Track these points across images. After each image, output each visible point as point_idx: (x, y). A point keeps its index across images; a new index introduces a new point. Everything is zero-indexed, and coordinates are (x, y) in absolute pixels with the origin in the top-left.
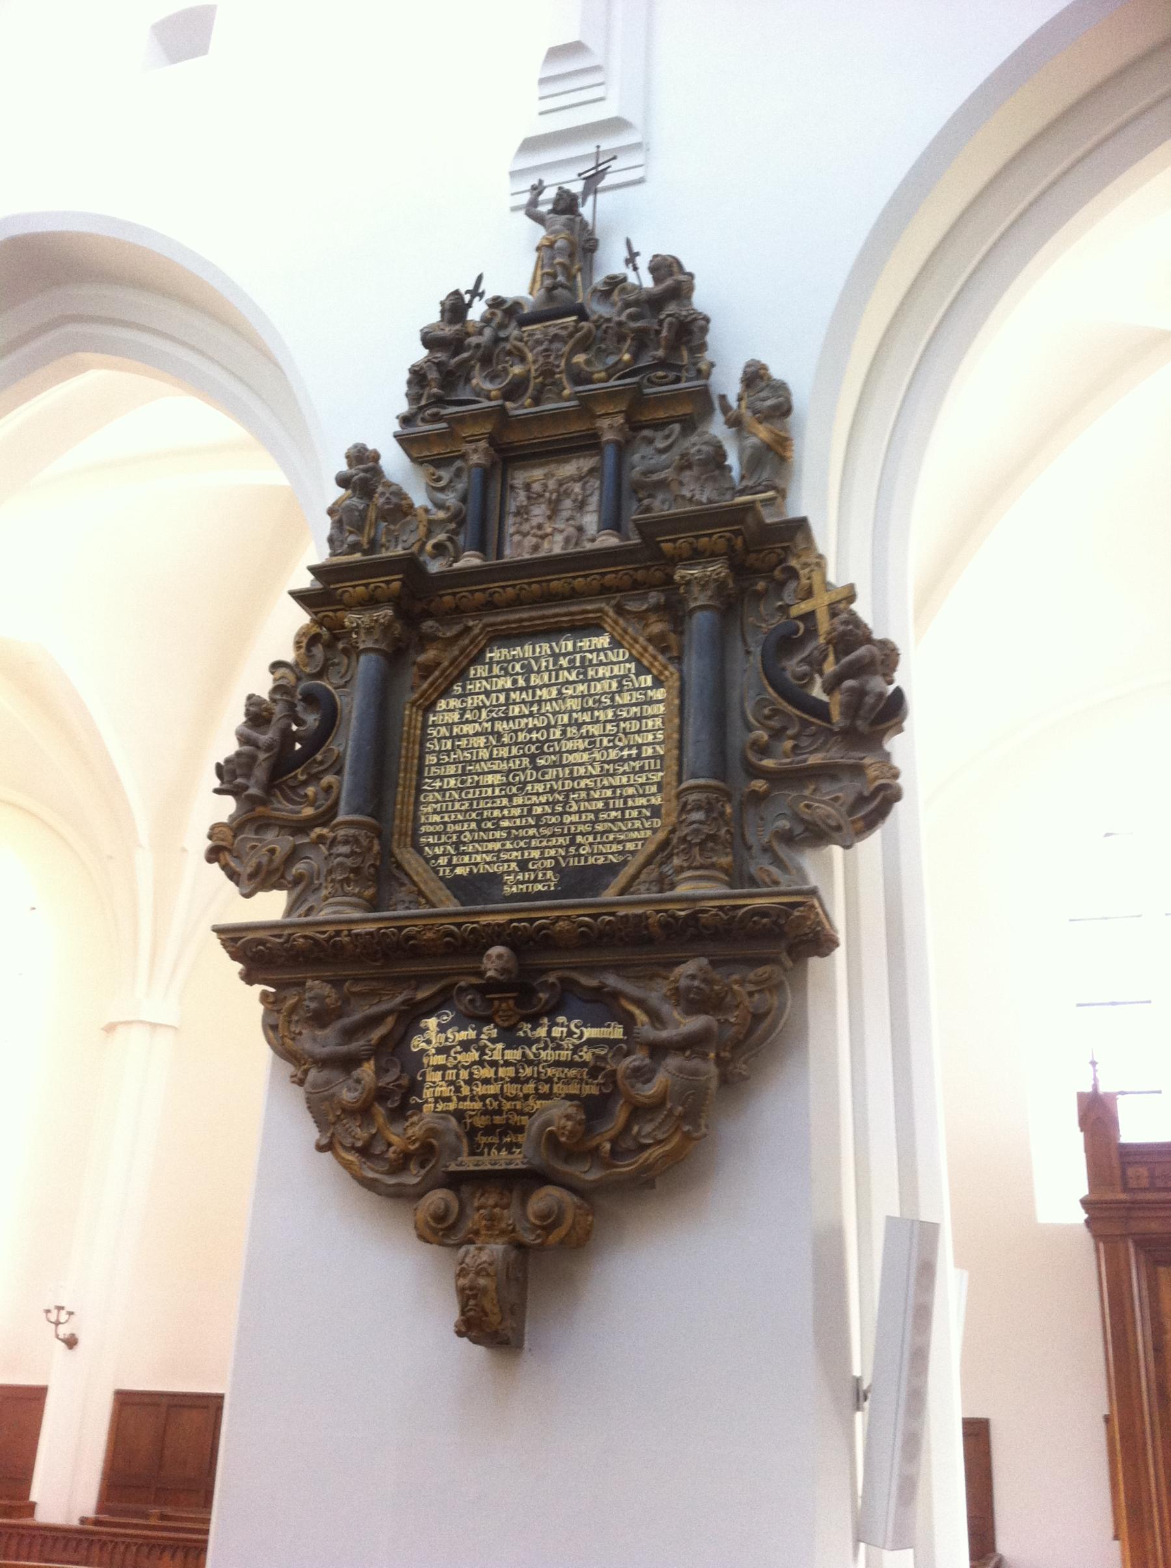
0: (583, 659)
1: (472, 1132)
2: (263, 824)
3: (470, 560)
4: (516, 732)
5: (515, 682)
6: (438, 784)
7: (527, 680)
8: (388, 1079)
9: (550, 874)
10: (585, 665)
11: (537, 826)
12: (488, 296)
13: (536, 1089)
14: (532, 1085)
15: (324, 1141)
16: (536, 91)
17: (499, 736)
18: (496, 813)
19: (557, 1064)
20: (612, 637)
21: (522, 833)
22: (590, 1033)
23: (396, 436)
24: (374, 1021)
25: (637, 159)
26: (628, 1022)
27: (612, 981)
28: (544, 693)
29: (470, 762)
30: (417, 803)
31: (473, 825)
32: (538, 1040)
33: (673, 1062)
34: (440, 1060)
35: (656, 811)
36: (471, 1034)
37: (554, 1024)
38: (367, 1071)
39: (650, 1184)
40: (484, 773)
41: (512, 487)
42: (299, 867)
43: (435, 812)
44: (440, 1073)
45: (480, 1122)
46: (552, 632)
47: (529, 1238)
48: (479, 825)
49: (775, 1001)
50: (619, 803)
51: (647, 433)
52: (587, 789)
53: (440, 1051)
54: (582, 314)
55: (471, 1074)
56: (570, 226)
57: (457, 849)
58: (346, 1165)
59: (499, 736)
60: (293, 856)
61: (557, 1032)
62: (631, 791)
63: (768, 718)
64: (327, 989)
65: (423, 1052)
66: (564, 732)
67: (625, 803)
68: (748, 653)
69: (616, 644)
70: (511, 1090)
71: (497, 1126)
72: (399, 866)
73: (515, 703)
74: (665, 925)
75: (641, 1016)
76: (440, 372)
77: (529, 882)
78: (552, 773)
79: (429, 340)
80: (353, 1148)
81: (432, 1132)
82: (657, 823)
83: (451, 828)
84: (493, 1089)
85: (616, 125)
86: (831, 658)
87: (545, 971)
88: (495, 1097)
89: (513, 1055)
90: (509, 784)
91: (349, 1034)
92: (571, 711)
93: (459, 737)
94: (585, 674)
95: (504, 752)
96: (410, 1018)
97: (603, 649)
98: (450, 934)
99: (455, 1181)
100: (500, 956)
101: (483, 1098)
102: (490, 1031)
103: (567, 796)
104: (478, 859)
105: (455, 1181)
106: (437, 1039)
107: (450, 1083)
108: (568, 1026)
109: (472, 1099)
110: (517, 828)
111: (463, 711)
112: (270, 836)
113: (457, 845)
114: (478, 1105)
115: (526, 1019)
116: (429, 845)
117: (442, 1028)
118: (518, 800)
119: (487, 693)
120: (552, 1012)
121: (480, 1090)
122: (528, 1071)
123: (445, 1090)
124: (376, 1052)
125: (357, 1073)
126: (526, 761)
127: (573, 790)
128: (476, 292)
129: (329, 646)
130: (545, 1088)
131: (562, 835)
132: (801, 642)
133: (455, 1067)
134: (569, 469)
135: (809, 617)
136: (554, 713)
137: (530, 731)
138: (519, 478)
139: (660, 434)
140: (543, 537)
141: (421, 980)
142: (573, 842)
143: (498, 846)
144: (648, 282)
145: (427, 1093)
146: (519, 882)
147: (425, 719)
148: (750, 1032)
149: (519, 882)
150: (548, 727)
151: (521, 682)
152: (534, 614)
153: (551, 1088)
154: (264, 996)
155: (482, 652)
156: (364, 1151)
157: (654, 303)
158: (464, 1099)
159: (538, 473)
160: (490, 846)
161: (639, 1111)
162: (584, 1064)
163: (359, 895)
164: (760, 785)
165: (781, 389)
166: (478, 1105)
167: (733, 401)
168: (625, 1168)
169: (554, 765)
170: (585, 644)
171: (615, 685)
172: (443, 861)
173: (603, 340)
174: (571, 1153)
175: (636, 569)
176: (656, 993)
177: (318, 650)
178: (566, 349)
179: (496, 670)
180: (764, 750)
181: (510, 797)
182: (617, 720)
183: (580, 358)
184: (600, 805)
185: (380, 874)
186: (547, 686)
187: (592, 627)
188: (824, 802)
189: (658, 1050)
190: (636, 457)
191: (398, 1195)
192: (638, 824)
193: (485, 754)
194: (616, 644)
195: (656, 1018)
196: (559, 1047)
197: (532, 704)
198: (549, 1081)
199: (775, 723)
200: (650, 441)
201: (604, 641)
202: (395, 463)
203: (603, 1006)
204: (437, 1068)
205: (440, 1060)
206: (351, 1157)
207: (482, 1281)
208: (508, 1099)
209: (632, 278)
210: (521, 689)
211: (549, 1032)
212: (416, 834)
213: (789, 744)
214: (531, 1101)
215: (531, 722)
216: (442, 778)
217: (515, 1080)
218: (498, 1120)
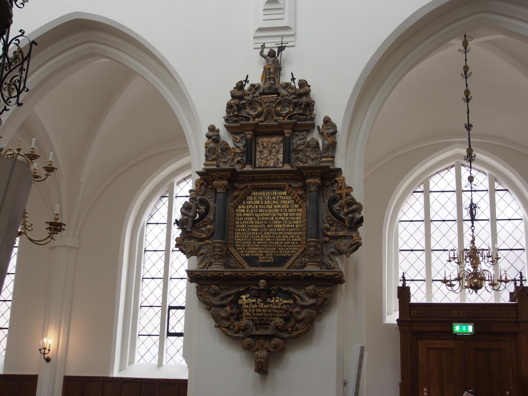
0: (279, 198)
1: (256, 325)
2: (191, 238)
3: (248, 168)
5: (260, 202)
6: (240, 230)
7: (264, 202)
8: (234, 311)
9: (271, 258)
10: (280, 200)
11: (268, 244)
12: (250, 83)
15: (217, 325)
16: (262, 12)
17: (256, 218)
18: (256, 239)
19: (277, 309)
20: (287, 192)
21: (263, 246)
22: (285, 302)
23: (224, 126)
24: (230, 295)
25: (292, 39)
26: (295, 300)
27: (291, 289)
29: (248, 224)
30: (234, 235)
31: (250, 242)
33: (306, 310)
34: (247, 306)
35: (300, 243)
36: (255, 301)
37: (276, 299)
38: (228, 308)
39: (299, 337)
41: (258, 143)
42: (202, 251)
43: (239, 238)
45: (258, 322)
46: (271, 189)
47: (271, 350)
49: (330, 295)
50: (290, 240)
51: (297, 133)
52: (281, 235)
53: (246, 304)
54: (279, 94)
56: (274, 62)
58: (223, 331)
59: (256, 218)
61: (277, 301)
62: (293, 237)
63: (329, 221)
64: (217, 287)
66: (274, 218)
68: (324, 201)
69: (288, 194)
70: (266, 315)
71: (262, 323)
72: (231, 253)
73: (260, 208)
74: (305, 277)
75: (298, 299)
76: (237, 107)
79: (233, 97)
80: (225, 327)
81: (247, 325)
82: (300, 246)
83: (244, 243)
84: (261, 314)
85: (287, 28)
86: (346, 207)
87: (274, 285)
88: (262, 316)
90: (259, 231)
91: (223, 299)
92: (276, 213)
94: (280, 202)
95: (258, 222)
96: (238, 295)
97: (285, 195)
98: (250, 276)
99: (252, 336)
100: (263, 283)
101: (259, 316)
102: (259, 300)
104: (252, 251)
105: (252, 336)
106: (246, 301)
107: (250, 312)
109: (256, 317)
111: (246, 209)
112: (192, 241)
113: (246, 247)
114: (257, 318)
115: (269, 297)
117: (247, 298)
119: (253, 205)
120: (275, 296)
121: (258, 314)
122: (270, 310)
123: (248, 314)
124: (230, 303)
125: (225, 309)
126: (264, 226)
127: (277, 235)
128: (246, 81)
129: (206, 187)
132: (338, 201)
134: (274, 139)
135: (340, 195)
136: (272, 213)
137: (265, 217)
138: (260, 140)
139: (300, 134)
140: (267, 161)
141: (240, 286)
142: (277, 249)
143: (257, 249)
144: (297, 87)
145: (244, 315)
146: (263, 259)
147: (235, 211)
148: (324, 303)
149: (263, 259)
150: (270, 216)
151: (262, 203)
154: (197, 287)
155: (251, 193)
157: (300, 95)
159: (265, 139)
160: (255, 249)
161: (298, 321)
162: (284, 309)
163: (222, 262)
164: (327, 239)
165: (334, 126)
166: (257, 318)
167: (321, 127)
168: (294, 334)
169: (272, 228)
170: (279, 193)
172: (242, 252)
173: (284, 102)
174: (281, 331)
176: (301, 293)
177: (203, 187)
179: (255, 198)
180: (328, 230)
182: (289, 216)
183: (278, 108)
185: (226, 256)
186: (269, 204)
187: (282, 189)
188: (343, 244)
189: (302, 307)
190: (294, 141)
191: (237, 338)
192: (295, 246)
194: (288, 194)
195: (302, 299)
196: (277, 305)
198: (275, 313)
199: (331, 222)
200: (298, 136)
201: (285, 193)
202: (224, 135)
203: (289, 295)
204: (246, 308)
205: (247, 306)
207: (262, 360)
209: (293, 84)
210: (262, 205)
212: (234, 244)
213: (335, 228)
216: (241, 228)
217: (267, 313)
218: (262, 322)
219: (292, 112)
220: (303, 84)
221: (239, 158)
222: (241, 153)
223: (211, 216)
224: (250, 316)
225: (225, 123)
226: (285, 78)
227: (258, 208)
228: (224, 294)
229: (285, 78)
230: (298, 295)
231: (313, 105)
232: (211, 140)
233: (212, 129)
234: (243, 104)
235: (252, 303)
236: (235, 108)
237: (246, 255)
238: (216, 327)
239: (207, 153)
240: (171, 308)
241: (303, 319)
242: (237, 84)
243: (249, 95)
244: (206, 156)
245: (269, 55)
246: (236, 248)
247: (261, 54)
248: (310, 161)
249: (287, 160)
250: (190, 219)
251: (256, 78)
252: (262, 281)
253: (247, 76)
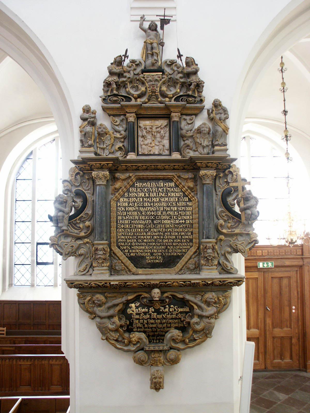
1: (148, 336)
3: (132, 156)
4: (146, 211)
5: (145, 195)
6: (123, 226)
7: (149, 194)
9: (160, 257)
10: (167, 192)
11: (155, 242)
13: (167, 326)
14: (165, 325)
17: (141, 212)
19: (172, 319)
20: (175, 183)
22: (180, 310)
24: (117, 305)
26: (192, 308)
28: (154, 199)
29: (133, 220)
31: (135, 240)
32: (166, 312)
34: (137, 317)
36: (147, 310)
37: (170, 307)
38: (116, 319)
40: (137, 224)
41: (140, 127)
42: (81, 251)
43: (122, 235)
44: (138, 321)
46: (157, 179)
48: (137, 241)
50: (180, 237)
51: (184, 117)
52: (170, 232)
53: (137, 314)
55: (147, 321)
57: (131, 247)
59: (141, 212)
60: (79, 248)
61: (171, 310)
62: (183, 234)
65: (131, 314)
66: (162, 213)
67: (182, 237)
69: (177, 186)
70: (160, 326)
73: (145, 202)
75: (195, 307)
76: (116, 85)
77: (154, 259)
78: (159, 226)
79: (112, 73)
82: (191, 244)
83: (128, 241)
84: (154, 326)
88: (155, 328)
89: (160, 316)
90: (146, 228)
91: (109, 308)
92: (164, 207)
93: (128, 211)
94: (167, 194)
96: (127, 304)
97: (173, 187)
100: (158, 293)
101: (152, 328)
103: (164, 234)
107: (141, 323)
108: (174, 308)
109: (148, 328)
110: (149, 242)
113: (131, 246)
114: (150, 330)
115: (162, 306)
116: (121, 245)
117: (137, 307)
118: (149, 234)
119: (136, 198)
121: (151, 326)
123: (139, 325)
127: (166, 232)
128: (126, 56)
129: (82, 176)
130: (169, 325)
131: (163, 245)
133: (142, 319)
137: (151, 212)
139: (188, 118)
142: (166, 248)
143: (144, 247)
144: (185, 65)
146: (151, 259)
147: (117, 204)
149: (151, 259)
150: (157, 211)
151: (147, 195)
152: (151, 174)
153: (171, 325)
157: (188, 75)
158: (146, 328)
160: (141, 247)
170: (167, 184)
171: (177, 199)
175: (185, 165)
177: (78, 177)
178: (159, 85)
179: (139, 190)
181: (146, 233)
182: (178, 211)
184: (174, 237)
187: (170, 180)
193: (137, 217)
194: (177, 186)
195: (199, 307)
196: (172, 314)
197: (151, 203)
198: (170, 323)
201: (173, 184)
204: (137, 319)
205: (137, 317)
206: (113, 342)
208: (159, 328)
209: (179, 61)
210: (147, 197)
211: (169, 310)
214: (165, 329)
215: (152, 209)
216: (124, 224)
217: (161, 323)
218: (156, 333)
219: (179, 93)
220: (190, 62)
221: (121, 145)
222: (122, 138)
223: (88, 210)
224: (141, 328)
225: (96, 104)
226: (169, 54)
227: (143, 202)
228: (110, 304)
229: (169, 54)
231: (203, 86)
232: (86, 122)
233: (87, 110)
234: (124, 82)
235: (143, 312)
236: (114, 86)
237: (132, 254)
239: (83, 138)
240: (38, 244)
242: (115, 59)
243: (129, 72)
244: (81, 141)
245: (150, 28)
246: (119, 248)
247: (141, 28)
248: (200, 149)
249: (175, 146)
250: (66, 216)
251: (136, 53)
253: (127, 51)
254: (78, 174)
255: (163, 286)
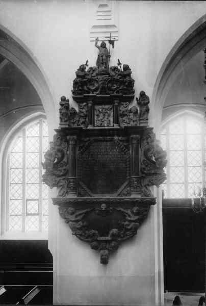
3: (90, 127)
8: (85, 224)
33: (133, 223)
54: (109, 74)
79: (78, 76)
81: (94, 233)
91: (76, 216)
128: (87, 65)
139: (124, 103)
144: (123, 70)
154: (59, 209)
156: (81, 235)
157: (125, 76)
164: (144, 175)
165: (148, 98)
167: (138, 99)
189: (130, 221)
200: (123, 105)
202: (73, 104)
206: (79, 236)
209: (119, 68)
219: (119, 88)
220: (126, 68)
221: (83, 120)
223: (65, 160)
226: (113, 63)
228: (77, 213)
229: (113, 63)
230: (127, 213)
231: (134, 83)
232: (63, 107)
233: (63, 99)
234: (85, 81)
236: (80, 84)
238: (73, 234)
239: (61, 116)
241: (131, 229)
242: (80, 67)
243: (88, 75)
245: (101, 46)
247: (96, 45)
248: (132, 123)
249: (116, 121)
250: (52, 163)
251: (93, 63)
252: (104, 205)
253: (87, 61)
254: (59, 138)
255: (108, 203)
